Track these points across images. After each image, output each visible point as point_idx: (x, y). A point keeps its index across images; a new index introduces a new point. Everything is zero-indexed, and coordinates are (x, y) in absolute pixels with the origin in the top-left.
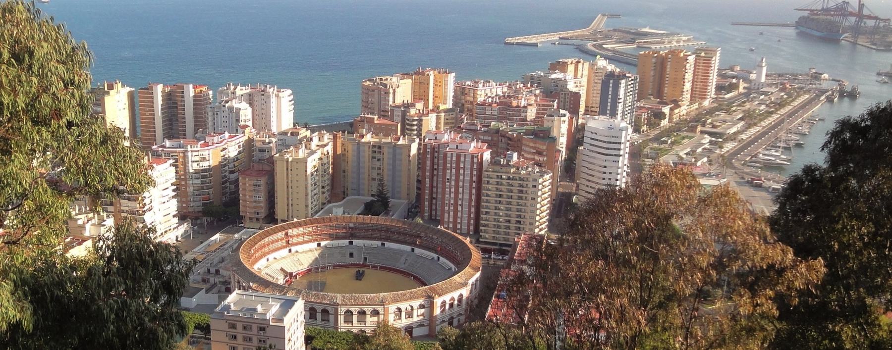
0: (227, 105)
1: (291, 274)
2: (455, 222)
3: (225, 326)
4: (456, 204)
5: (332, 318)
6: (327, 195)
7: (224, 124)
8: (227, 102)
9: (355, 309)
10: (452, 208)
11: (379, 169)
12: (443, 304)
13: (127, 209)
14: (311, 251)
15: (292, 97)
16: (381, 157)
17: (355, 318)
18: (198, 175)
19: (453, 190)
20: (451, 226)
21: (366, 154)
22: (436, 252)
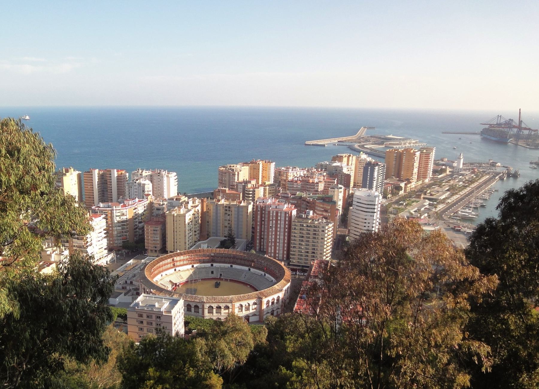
0: (137, 182)
1: (176, 284)
2: (275, 253)
3: (136, 316)
4: (275, 242)
5: (200, 310)
6: (197, 236)
7: (135, 193)
8: (137, 180)
9: (214, 305)
10: (273, 244)
12: (268, 302)
13: (77, 244)
14: (188, 270)
15: (176, 177)
16: (230, 213)
17: (214, 311)
18: (120, 224)
19: (274, 233)
20: (272, 255)
21: (221, 211)
22: (264, 271)
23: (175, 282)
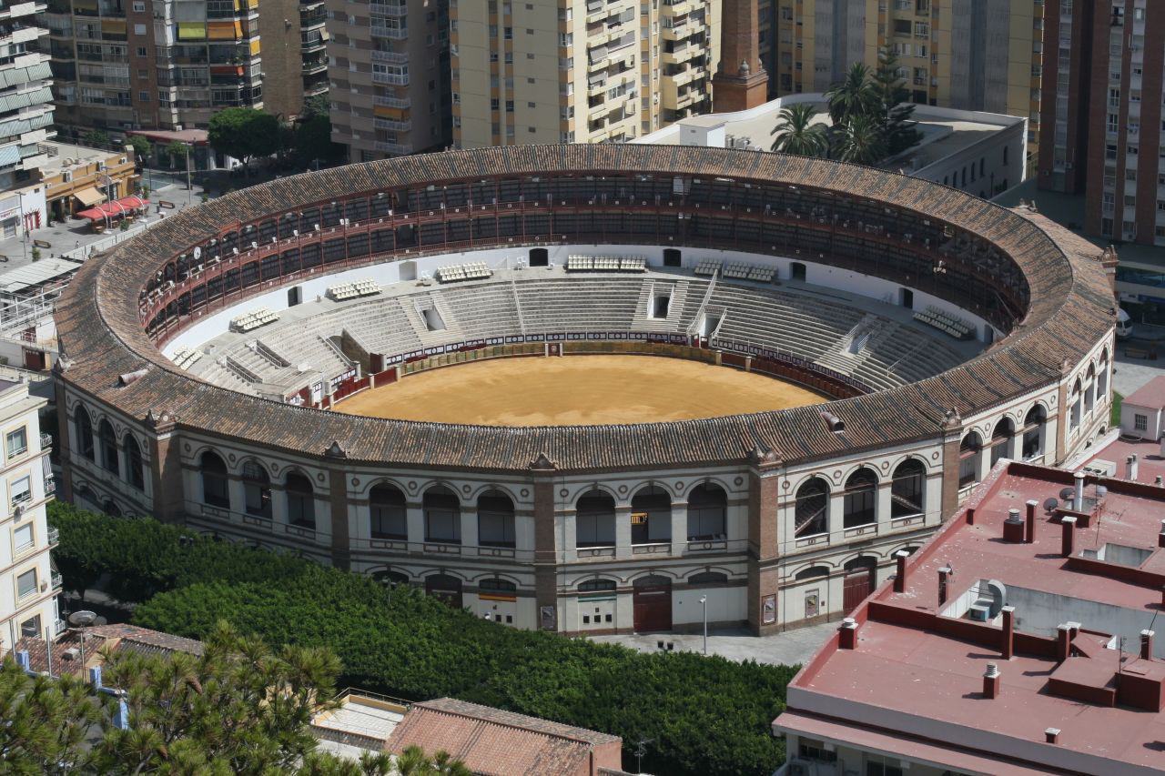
10: (1134, 139)
23: (370, 348)
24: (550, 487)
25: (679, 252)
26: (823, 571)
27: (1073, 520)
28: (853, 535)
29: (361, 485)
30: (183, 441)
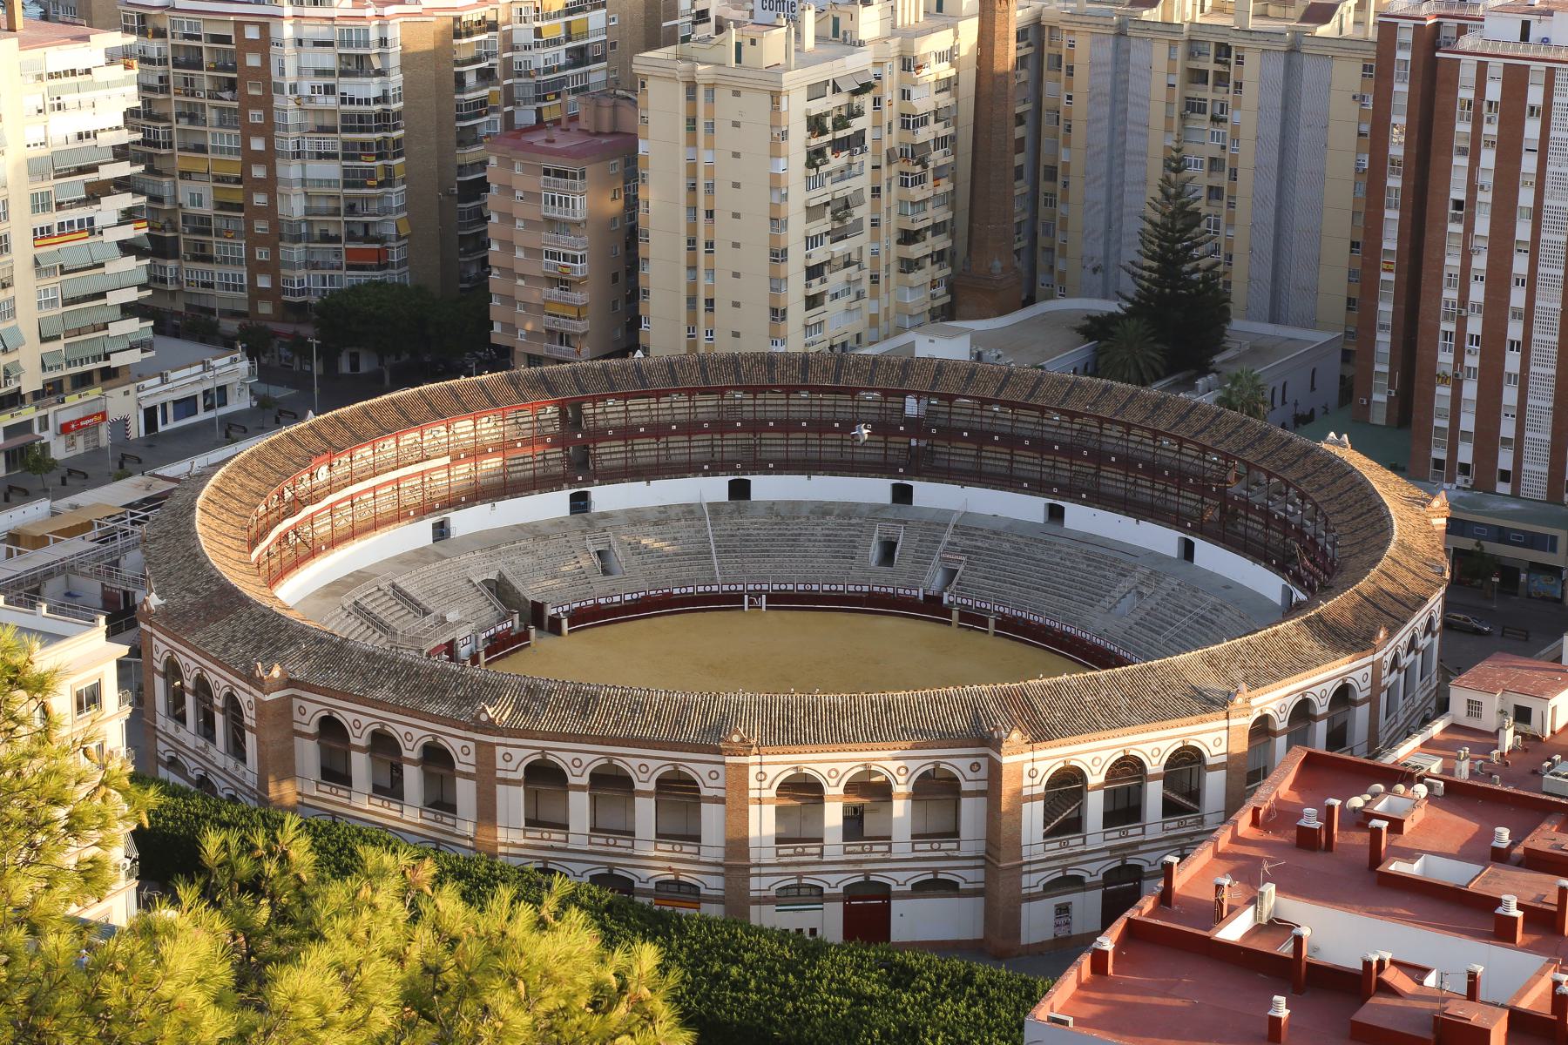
2: (1486, 438)
4: (1493, 343)
5: (465, 793)
6: (930, 271)
9: (578, 763)
10: (1472, 361)
11: (1215, 164)
19: (1480, 263)
20: (1466, 454)
24: (746, 766)
25: (911, 487)
26: (1076, 883)
27: (1384, 824)
28: (1115, 837)
29: (514, 758)
30: (296, 703)
